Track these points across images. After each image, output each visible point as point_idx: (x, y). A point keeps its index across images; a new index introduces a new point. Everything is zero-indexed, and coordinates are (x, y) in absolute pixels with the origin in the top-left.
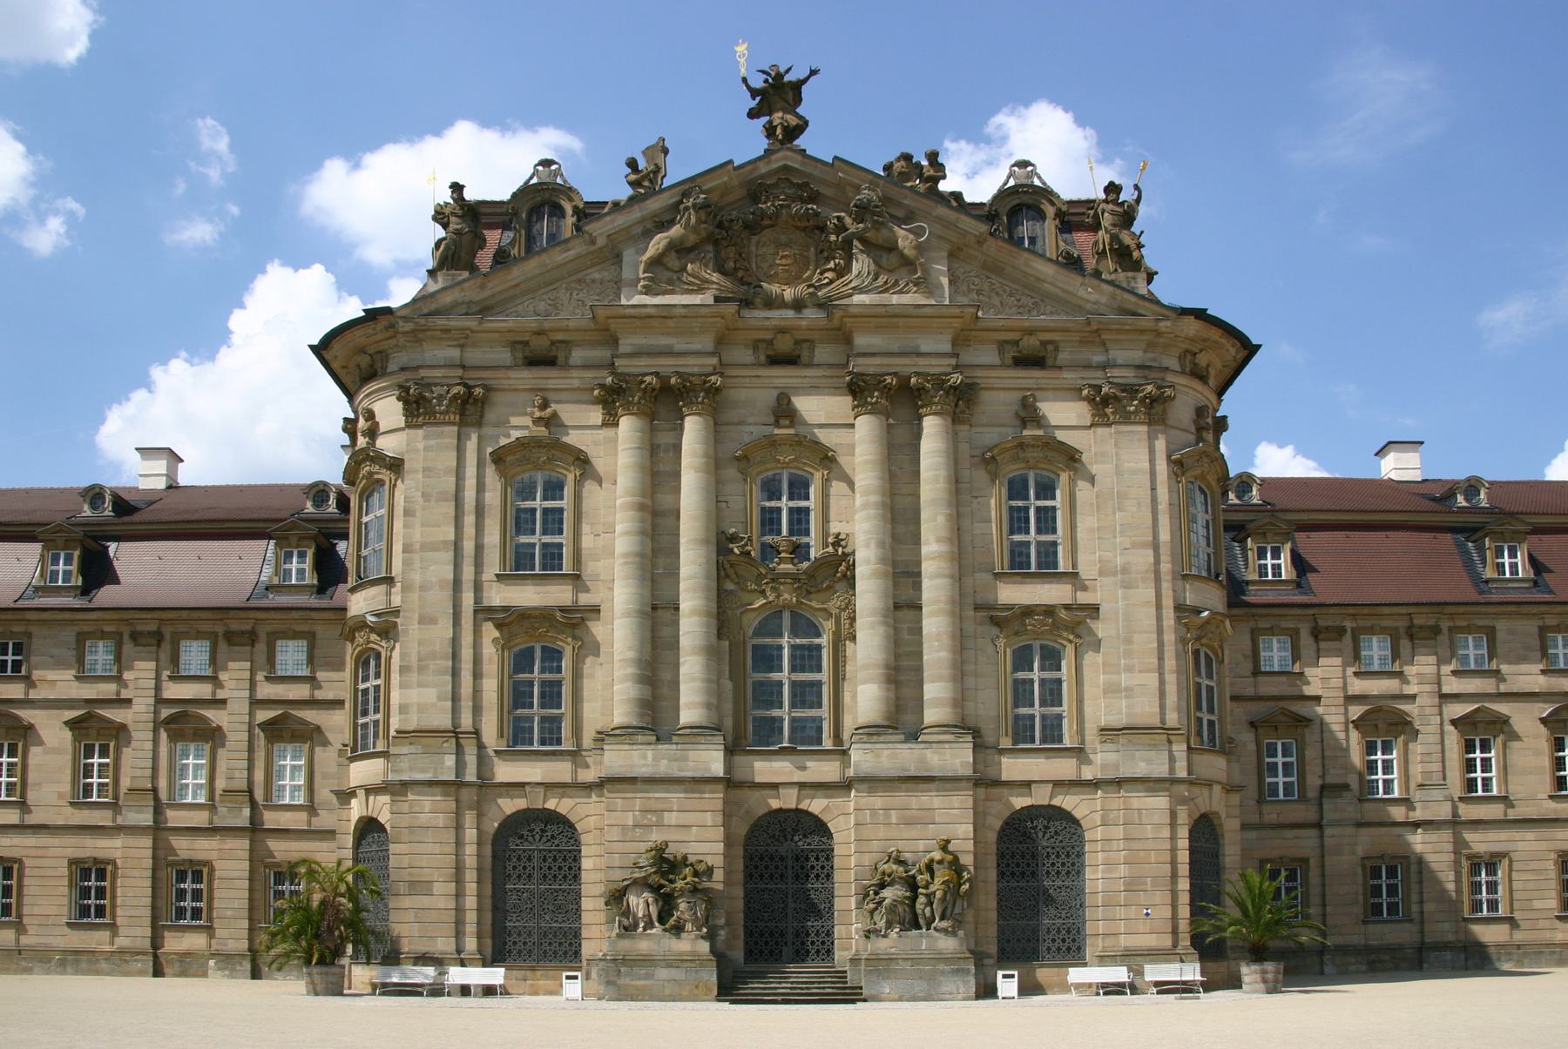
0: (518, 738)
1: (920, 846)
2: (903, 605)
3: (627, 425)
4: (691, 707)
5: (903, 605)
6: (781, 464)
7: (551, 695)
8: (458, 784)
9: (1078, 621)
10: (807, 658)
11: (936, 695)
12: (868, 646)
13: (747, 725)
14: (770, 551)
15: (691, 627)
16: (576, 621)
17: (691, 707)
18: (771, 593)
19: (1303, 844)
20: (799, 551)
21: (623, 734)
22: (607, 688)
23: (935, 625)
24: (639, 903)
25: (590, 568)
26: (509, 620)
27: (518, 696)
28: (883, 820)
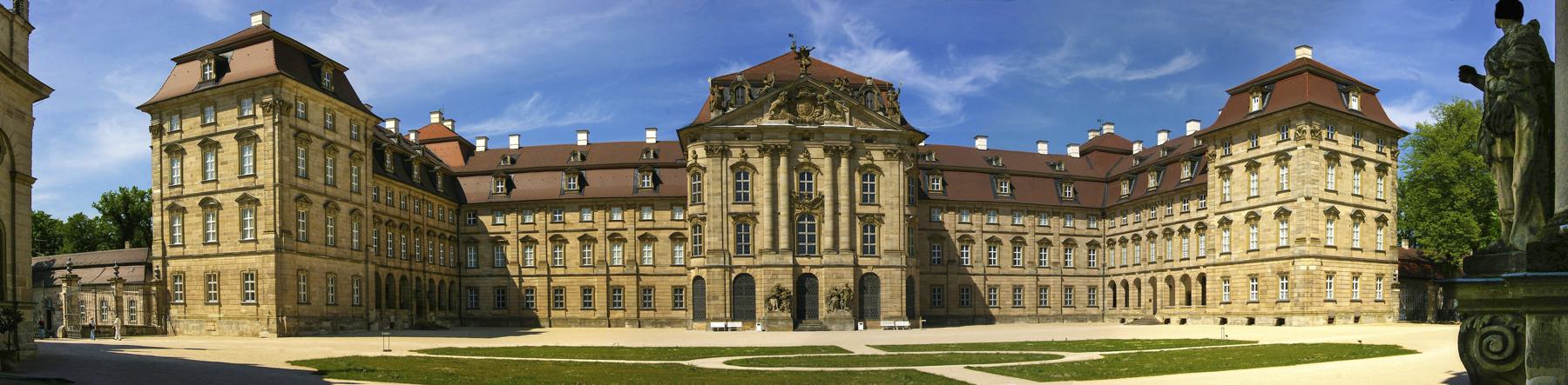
0: (738, 250)
1: (841, 285)
2: (836, 214)
3: (766, 159)
4: (783, 243)
5: (836, 214)
6: (805, 172)
7: (747, 239)
8: (724, 267)
9: (880, 218)
10: (812, 228)
11: (844, 240)
12: (827, 226)
13: (797, 248)
14: (802, 196)
15: (783, 220)
16: (753, 216)
17: (783, 243)
18: (803, 208)
19: (942, 280)
20: (810, 196)
21: (768, 251)
22: (761, 238)
23: (844, 220)
24: (773, 301)
25: (757, 200)
26: (736, 216)
27: (738, 238)
28: (831, 277)
